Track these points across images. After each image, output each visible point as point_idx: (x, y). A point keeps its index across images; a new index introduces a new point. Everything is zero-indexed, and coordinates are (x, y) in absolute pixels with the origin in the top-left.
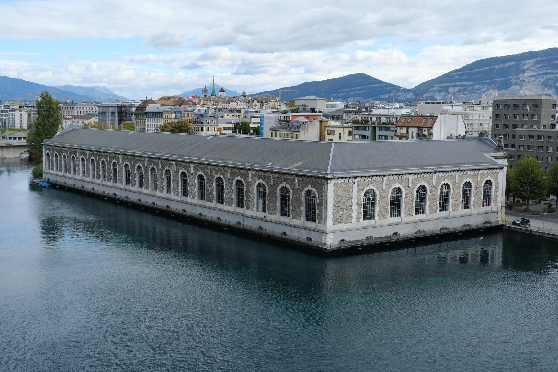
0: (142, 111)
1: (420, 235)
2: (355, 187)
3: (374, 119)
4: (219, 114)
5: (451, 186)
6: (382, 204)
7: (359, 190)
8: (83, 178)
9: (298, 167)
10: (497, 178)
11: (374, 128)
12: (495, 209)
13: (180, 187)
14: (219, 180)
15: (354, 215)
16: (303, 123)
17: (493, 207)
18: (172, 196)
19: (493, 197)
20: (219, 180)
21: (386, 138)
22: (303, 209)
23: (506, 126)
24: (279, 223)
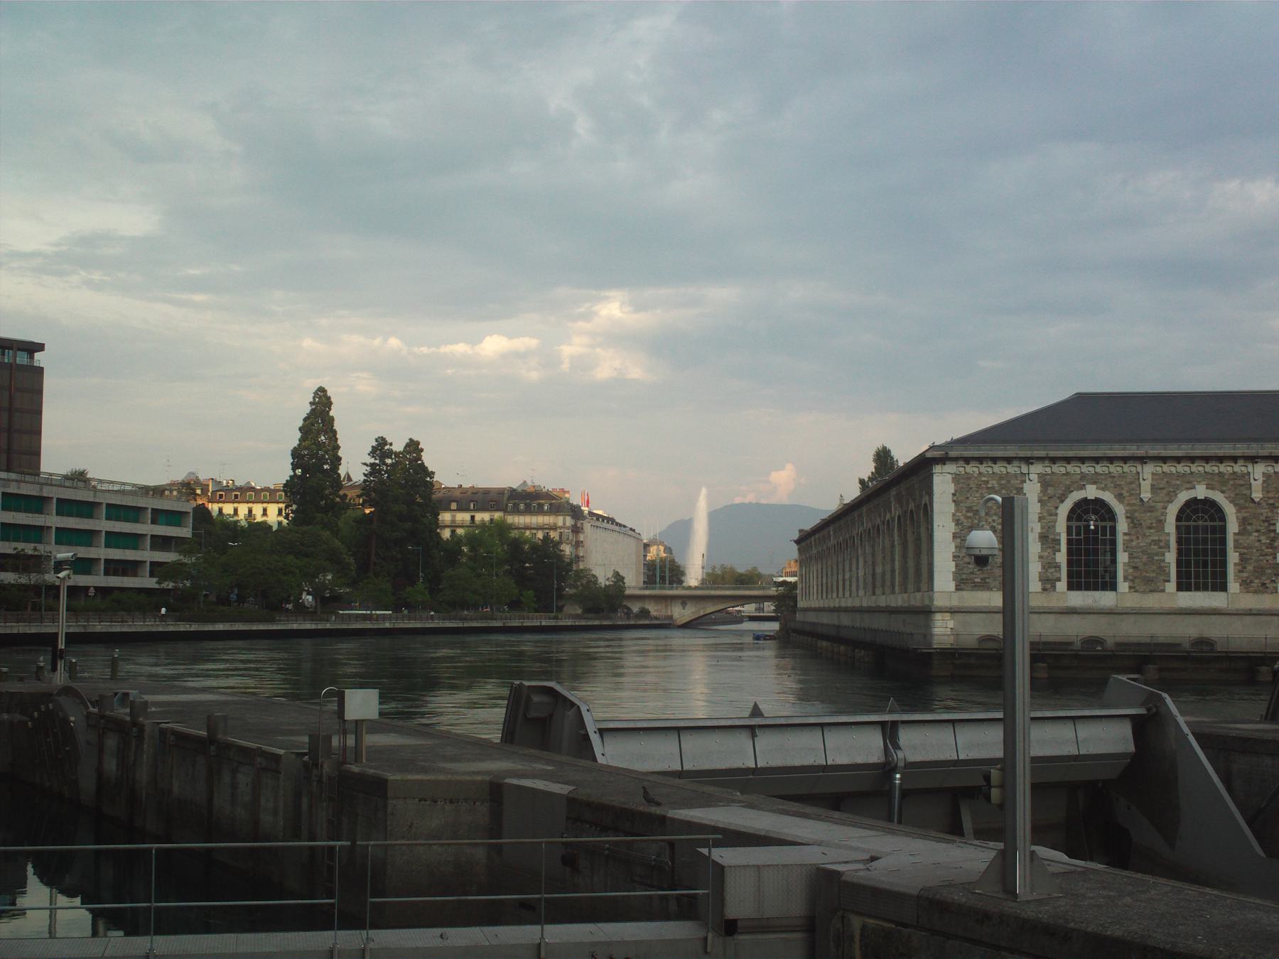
2: (1032, 490)
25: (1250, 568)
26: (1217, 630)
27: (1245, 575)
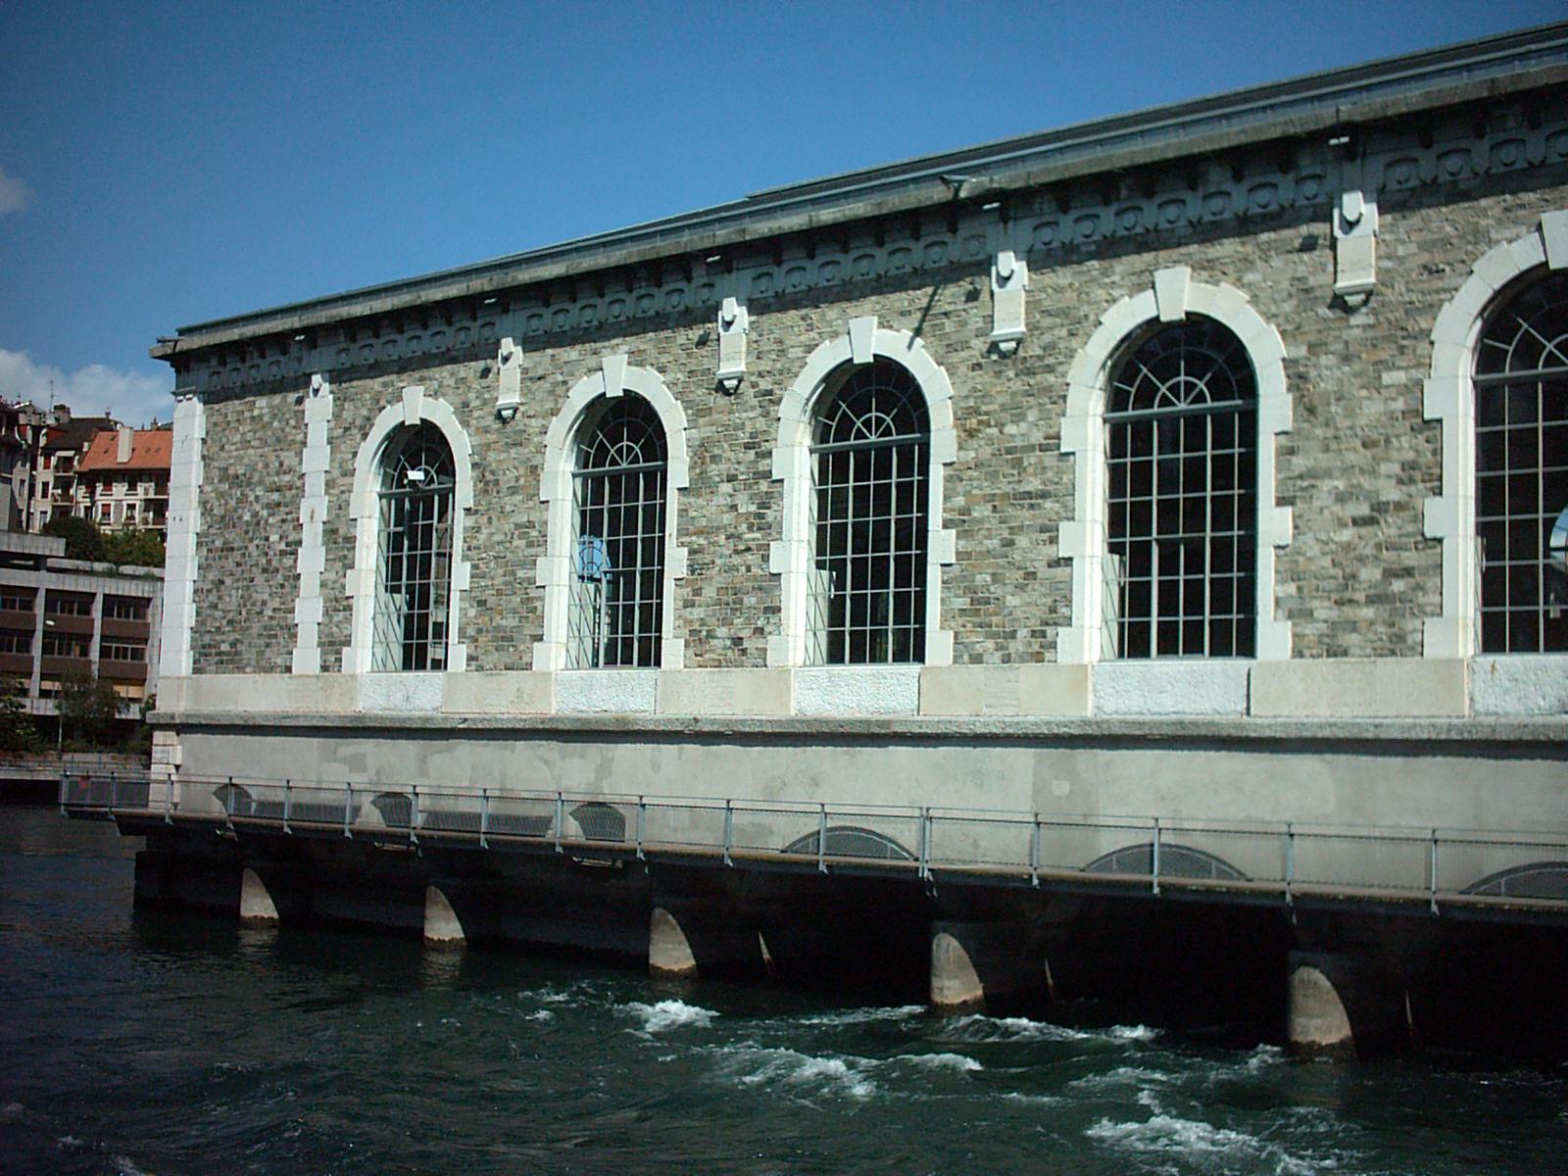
7: (346, 432)
25: (709, 592)
26: (628, 775)
27: (697, 613)
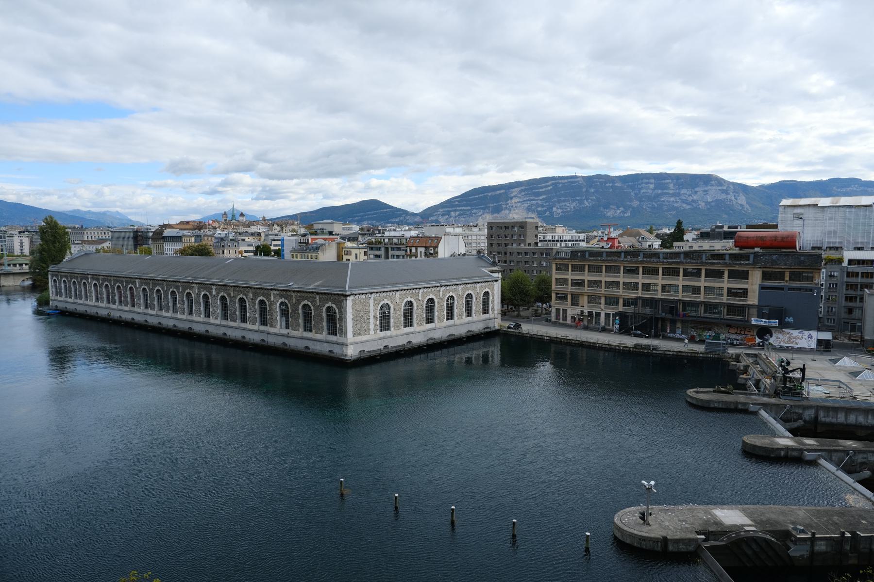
0: (159, 236)
1: (431, 342)
2: (372, 302)
3: (386, 240)
4: (240, 238)
5: (456, 298)
6: (397, 316)
8: (97, 304)
9: (318, 286)
10: (493, 290)
11: (387, 248)
12: (492, 316)
13: (202, 308)
14: (242, 300)
15: (372, 327)
16: (322, 245)
17: (491, 315)
18: (194, 318)
19: (491, 305)
20: (242, 300)
21: (398, 257)
22: (325, 324)
23: (499, 245)
24: (302, 338)
